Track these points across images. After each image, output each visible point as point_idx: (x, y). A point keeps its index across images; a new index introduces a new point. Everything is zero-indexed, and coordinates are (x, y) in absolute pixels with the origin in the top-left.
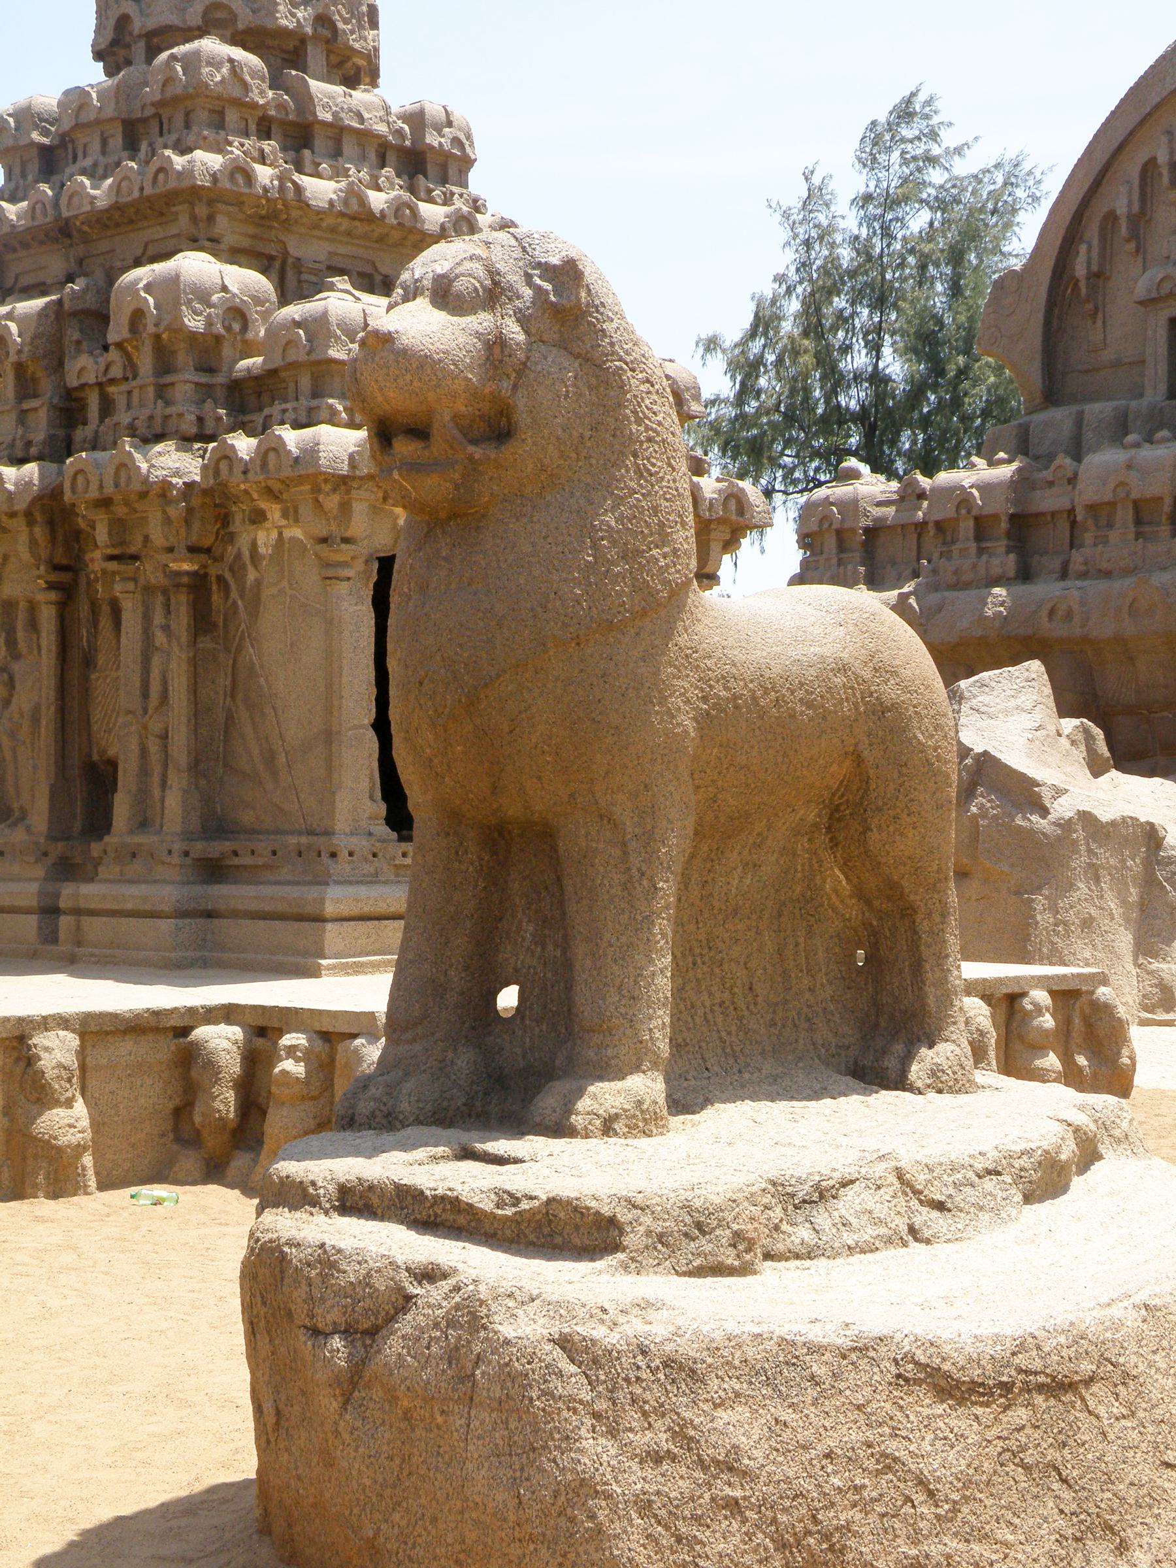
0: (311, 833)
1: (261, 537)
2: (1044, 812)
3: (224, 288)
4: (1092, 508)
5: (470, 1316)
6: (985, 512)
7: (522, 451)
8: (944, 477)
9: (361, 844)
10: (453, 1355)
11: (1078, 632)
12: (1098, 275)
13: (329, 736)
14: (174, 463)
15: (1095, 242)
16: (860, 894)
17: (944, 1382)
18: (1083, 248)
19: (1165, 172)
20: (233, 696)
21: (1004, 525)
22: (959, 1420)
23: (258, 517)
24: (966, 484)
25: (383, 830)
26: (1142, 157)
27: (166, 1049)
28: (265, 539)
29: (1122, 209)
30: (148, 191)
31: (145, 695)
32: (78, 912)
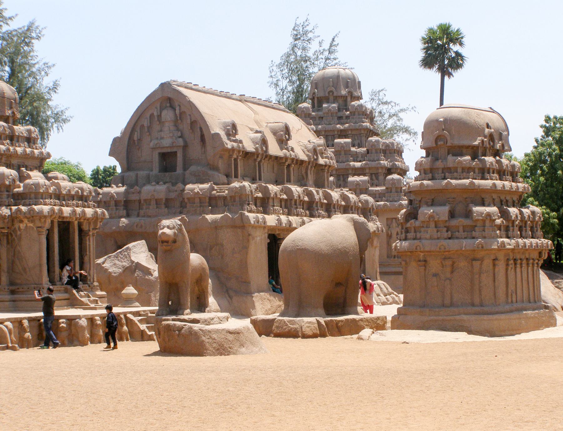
0: (36, 284)
2: (152, 275)
3: (11, 175)
4: (145, 200)
6: (118, 199)
7: (177, 244)
8: (106, 190)
10: (189, 331)
13: (41, 265)
15: (139, 131)
16: (199, 290)
17: (230, 333)
18: (136, 133)
19: (156, 117)
20: (14, 257)
21: (123, 203)
23: (21, 221)
24: (112, 192)
25: (49, 283)
26: (150, 112)
27: (38, 323)
28: (22, 226)
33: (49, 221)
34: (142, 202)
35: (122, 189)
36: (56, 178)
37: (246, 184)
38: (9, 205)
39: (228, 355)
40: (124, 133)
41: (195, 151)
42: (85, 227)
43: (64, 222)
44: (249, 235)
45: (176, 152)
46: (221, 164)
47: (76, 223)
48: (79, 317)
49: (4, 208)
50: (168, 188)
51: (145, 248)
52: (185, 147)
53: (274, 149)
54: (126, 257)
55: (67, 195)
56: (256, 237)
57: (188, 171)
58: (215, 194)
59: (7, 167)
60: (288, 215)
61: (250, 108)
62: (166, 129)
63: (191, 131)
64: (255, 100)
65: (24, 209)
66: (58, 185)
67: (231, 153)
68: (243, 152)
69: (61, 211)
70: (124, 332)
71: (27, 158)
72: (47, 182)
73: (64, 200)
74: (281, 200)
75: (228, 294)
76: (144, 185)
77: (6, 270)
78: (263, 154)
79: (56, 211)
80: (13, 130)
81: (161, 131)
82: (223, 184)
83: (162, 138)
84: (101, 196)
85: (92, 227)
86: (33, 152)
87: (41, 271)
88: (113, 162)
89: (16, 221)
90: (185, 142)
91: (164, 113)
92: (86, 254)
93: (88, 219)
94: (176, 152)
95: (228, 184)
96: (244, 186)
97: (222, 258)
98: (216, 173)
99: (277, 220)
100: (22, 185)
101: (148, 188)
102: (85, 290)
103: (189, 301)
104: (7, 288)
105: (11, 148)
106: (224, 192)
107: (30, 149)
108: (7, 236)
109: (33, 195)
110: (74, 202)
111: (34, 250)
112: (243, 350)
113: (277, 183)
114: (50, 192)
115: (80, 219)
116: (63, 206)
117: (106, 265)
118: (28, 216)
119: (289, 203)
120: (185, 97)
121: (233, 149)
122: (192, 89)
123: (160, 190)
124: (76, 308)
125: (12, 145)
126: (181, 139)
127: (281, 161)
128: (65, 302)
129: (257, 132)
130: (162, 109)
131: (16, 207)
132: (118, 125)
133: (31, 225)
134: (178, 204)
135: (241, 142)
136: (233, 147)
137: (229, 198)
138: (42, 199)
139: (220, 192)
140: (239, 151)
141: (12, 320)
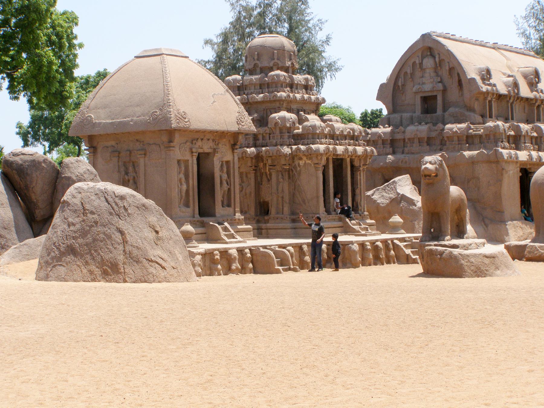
0: (314, 214)
1: (301, 162)
2: (416, 206)
4: (409, 139)
5: (451, 252)
8: (374, 130)
9: (324, 215)
11: (408, 166)
12: (403, 85)
13: (318, 197)
14: (286, 150)
16: (458, 219)
17: (486, 257)
18: (400, 79)
21: (389, 142)
22: (487, 259)
23: (301, 159)
24: (380, 132)
25: (325, 213)
29: (409, 72)
30: (272, 99)
31: (278, 190)
32: (267, 229)
33: (324, 158)
34: (407, 141)
35: (389, 129)
36: (331, 120)
37: (500, 123)
38: (290, 145)
39: (485, 277)
40: (389, 80)
41: (453, 94)
42: (356, 164)
43: (338, 159)
44: (503, 169)
45: (436, 96)
46: (477, 106)
47: (348, 160)
48: (352, 243)
49: (285, 147)
50: (429, 128)
51: (409, 181)
52: (445, 91)
53: (525, 91)
54: (393, 190)
55: (340, 135)
56: (509, 171)
57: (447, 113)
58: (471, 133)
59: (288, 111)
60: (538, 151)
61: (502, 54)
62: (427, 75)
63: (449, 77)
64: (507, 48)
65: (302, 147)
66: (332, 127)
67: (486, 96)
68: (497, 94)
69: (335, 149)
70: (392, 256)
71: (305, 103)
72: (323, 124)
73: (338, 140)
74: (532, 138)
75: (484, 222)
76: (408, 125)
77: (288, 202)
78: (514, 97)
79: (331, 149)
80: (292, 79)
81: (422, 77)
82: (479, 124)
83: (424, 83)
84: (370, 136)
85: (362, 163)
86: (310, 98)
87: (318, 201)
88: (380, 106)
89: (296, 159)
90: (444, 86)
91: (425, 61)
92: (358, 187)
93: (359, 156)
94: (436, 96)
95: (484, 124)
96: (498, 125)
97: (478, 189)
98: (472, 114)
99: (529, 155)
100: (301, 127)
101: (411, 129)
102: (357, 219)
103: (449, 228)
104: (288, 217)
105: (291, 95)
106: (480, 131)
107: (307, 95)
108: (289, 171)
109: (310, 136)
110: (347, 141)
111: (312, 183)
112: (498, 272)
113: (528, 122)
114: (326, 132)
115: (352, 156)
116: (337, 145)
117: (375, 197)
118: (307, 154)
119: (539, 140)
120: (444, 46)
121: (487, 92)
122: (449, 39)
123: (423, 130)
124: (349, 235)
125: (292, 92)
126: (440, 84)
127: (532, 102)
129: (509, 76)
130: (423, 58)
131: (296, 146)
132: (384, 72)
133: (309, 162)
134: (438, 142)
135: (494, 85)
136: (487, 90)
137: (484, 137)
138: (318, 139)
139: (476, 131)
140: (493, 94)
141: (294, 246)
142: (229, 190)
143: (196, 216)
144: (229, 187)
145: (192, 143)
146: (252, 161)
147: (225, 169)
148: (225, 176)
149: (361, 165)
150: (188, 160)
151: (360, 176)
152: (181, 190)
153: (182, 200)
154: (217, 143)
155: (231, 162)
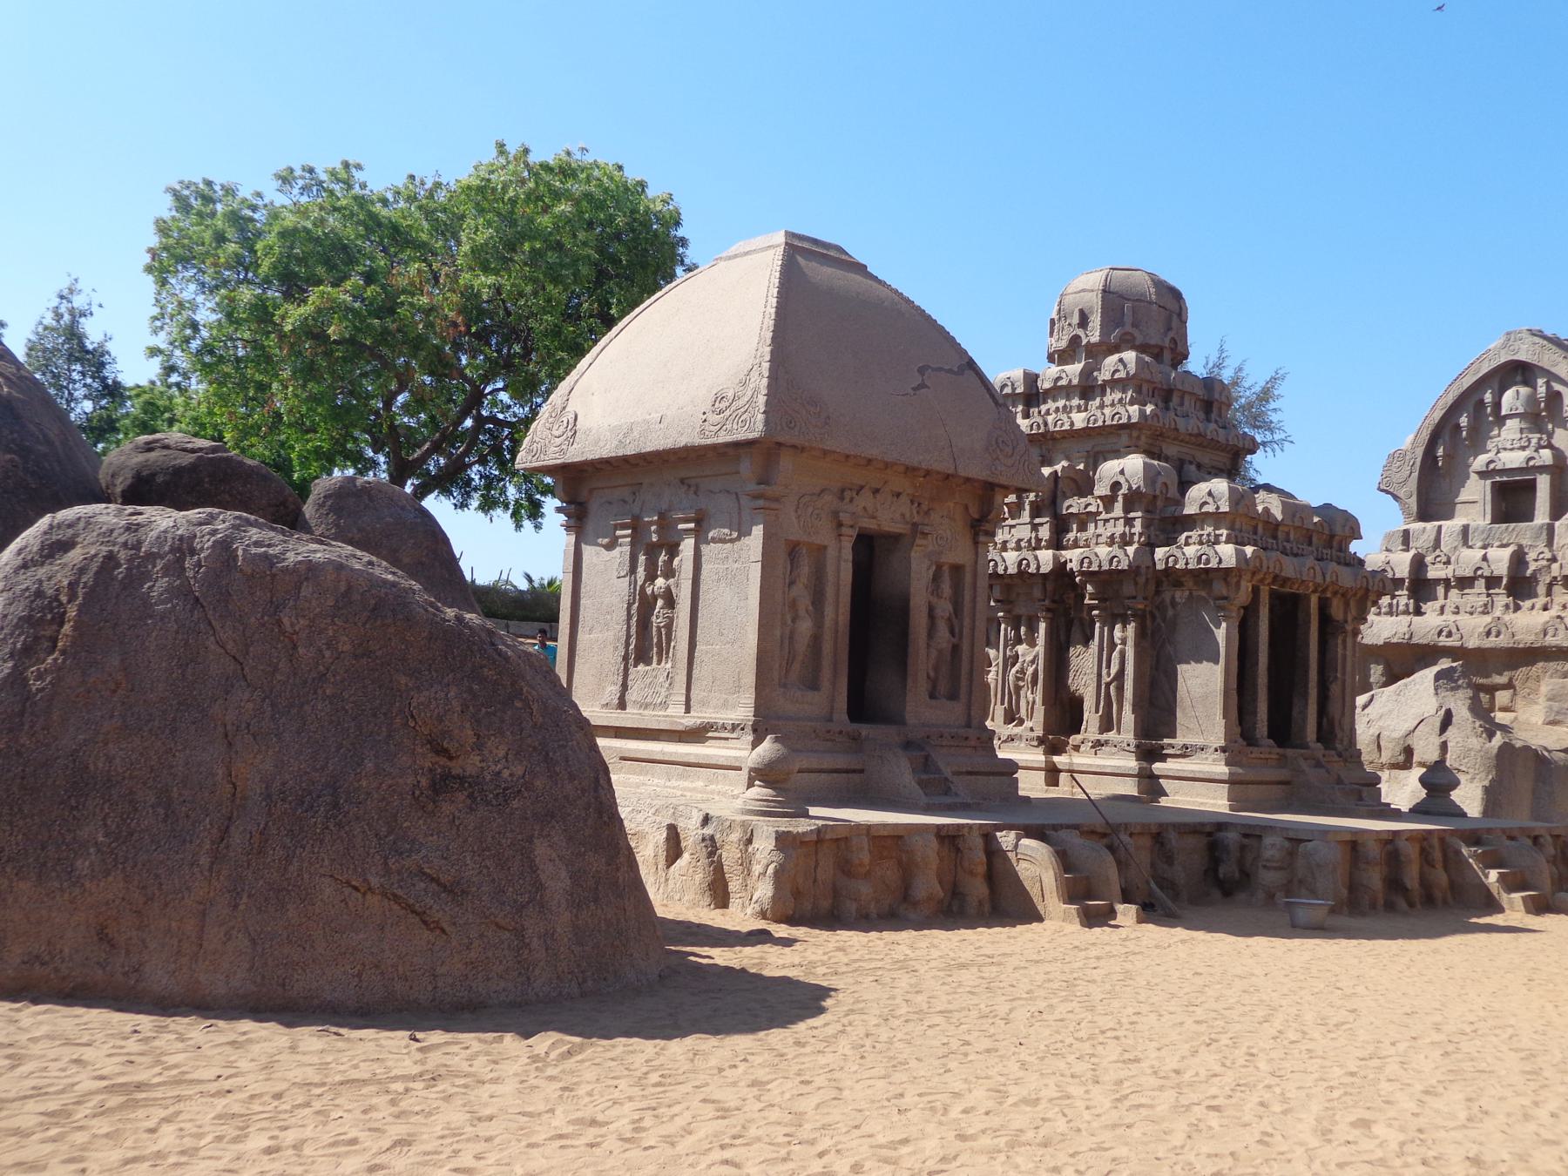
1: (1178, 594)
11: (1458, 644)
23: (1178, 584)
26: (1475, 398)
27: (1204, 840)
33: (1246, 586)
47: (1314, 599)
115: (1324, 591)
128: (1276, 790)
142: (956, 649)
143: (835, 717)
144: (955, 641)
145: (842, 499)
146: (1044, 585)
147: (946, 588)
148: (944, 608)
149: (1350, 619)
150: (825, 547)
151: (1345, 648)
152: (792, 633)
153: (796, 666)
154: (924, 507)
155: (968, 570)
